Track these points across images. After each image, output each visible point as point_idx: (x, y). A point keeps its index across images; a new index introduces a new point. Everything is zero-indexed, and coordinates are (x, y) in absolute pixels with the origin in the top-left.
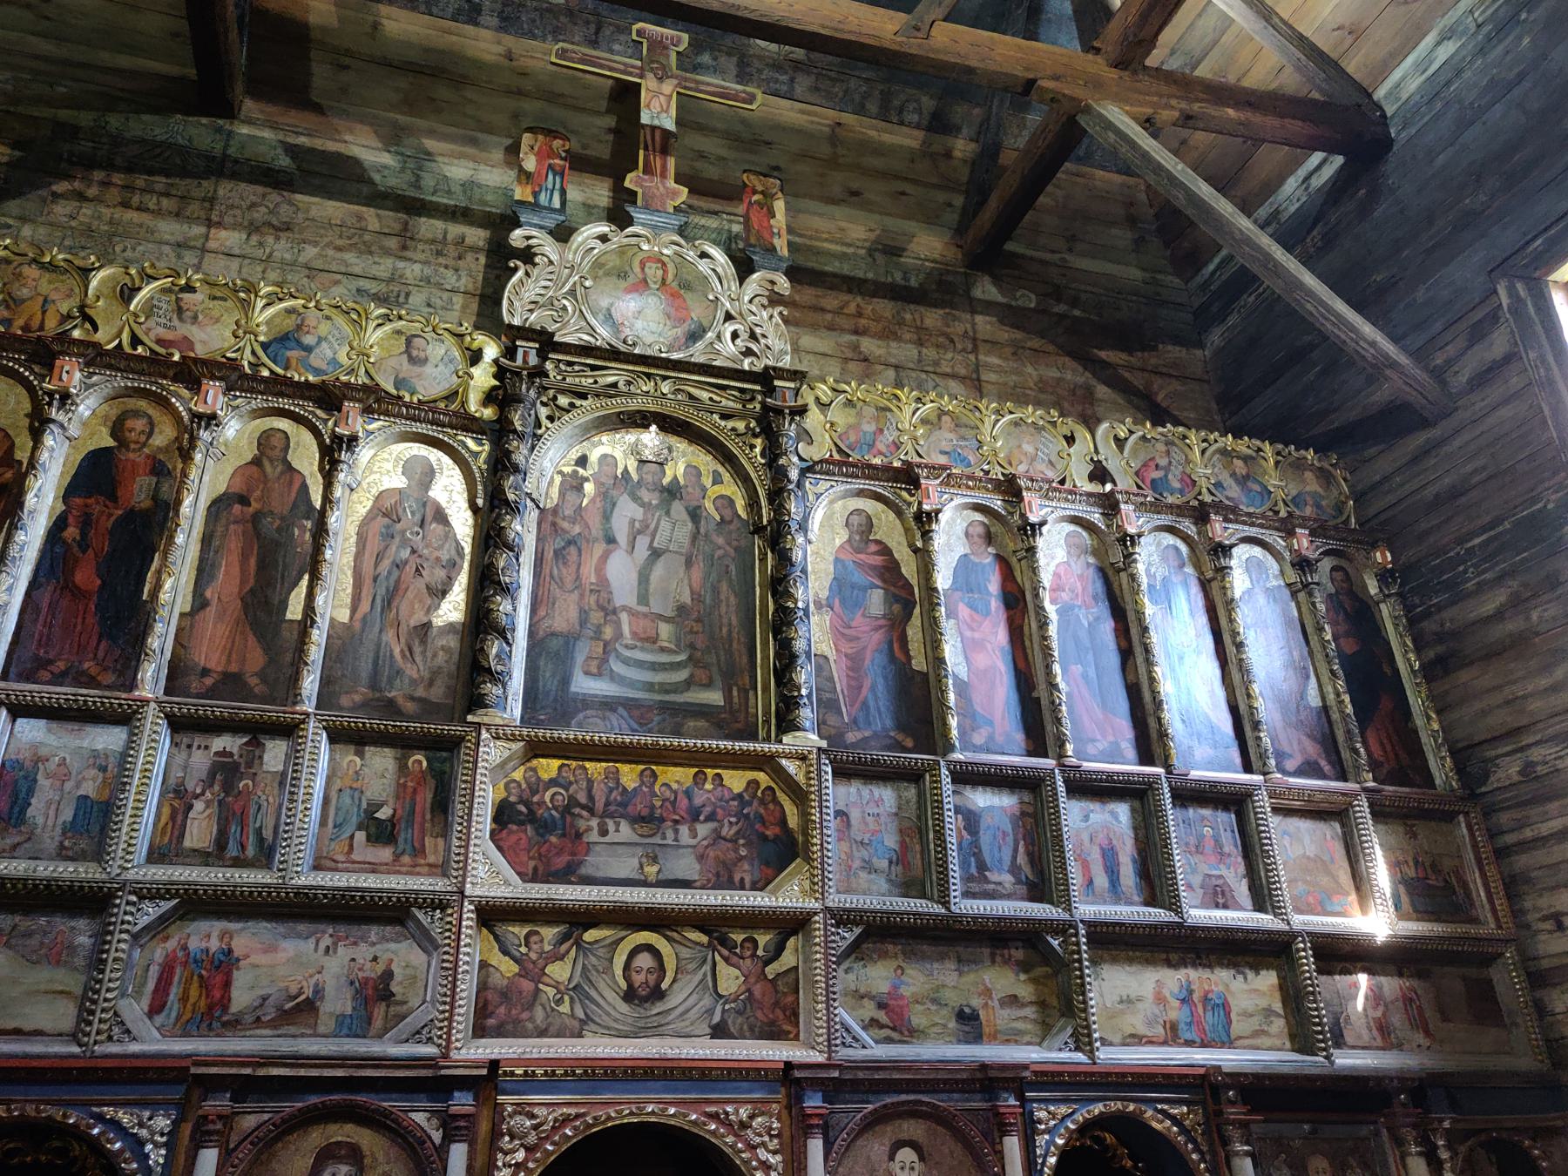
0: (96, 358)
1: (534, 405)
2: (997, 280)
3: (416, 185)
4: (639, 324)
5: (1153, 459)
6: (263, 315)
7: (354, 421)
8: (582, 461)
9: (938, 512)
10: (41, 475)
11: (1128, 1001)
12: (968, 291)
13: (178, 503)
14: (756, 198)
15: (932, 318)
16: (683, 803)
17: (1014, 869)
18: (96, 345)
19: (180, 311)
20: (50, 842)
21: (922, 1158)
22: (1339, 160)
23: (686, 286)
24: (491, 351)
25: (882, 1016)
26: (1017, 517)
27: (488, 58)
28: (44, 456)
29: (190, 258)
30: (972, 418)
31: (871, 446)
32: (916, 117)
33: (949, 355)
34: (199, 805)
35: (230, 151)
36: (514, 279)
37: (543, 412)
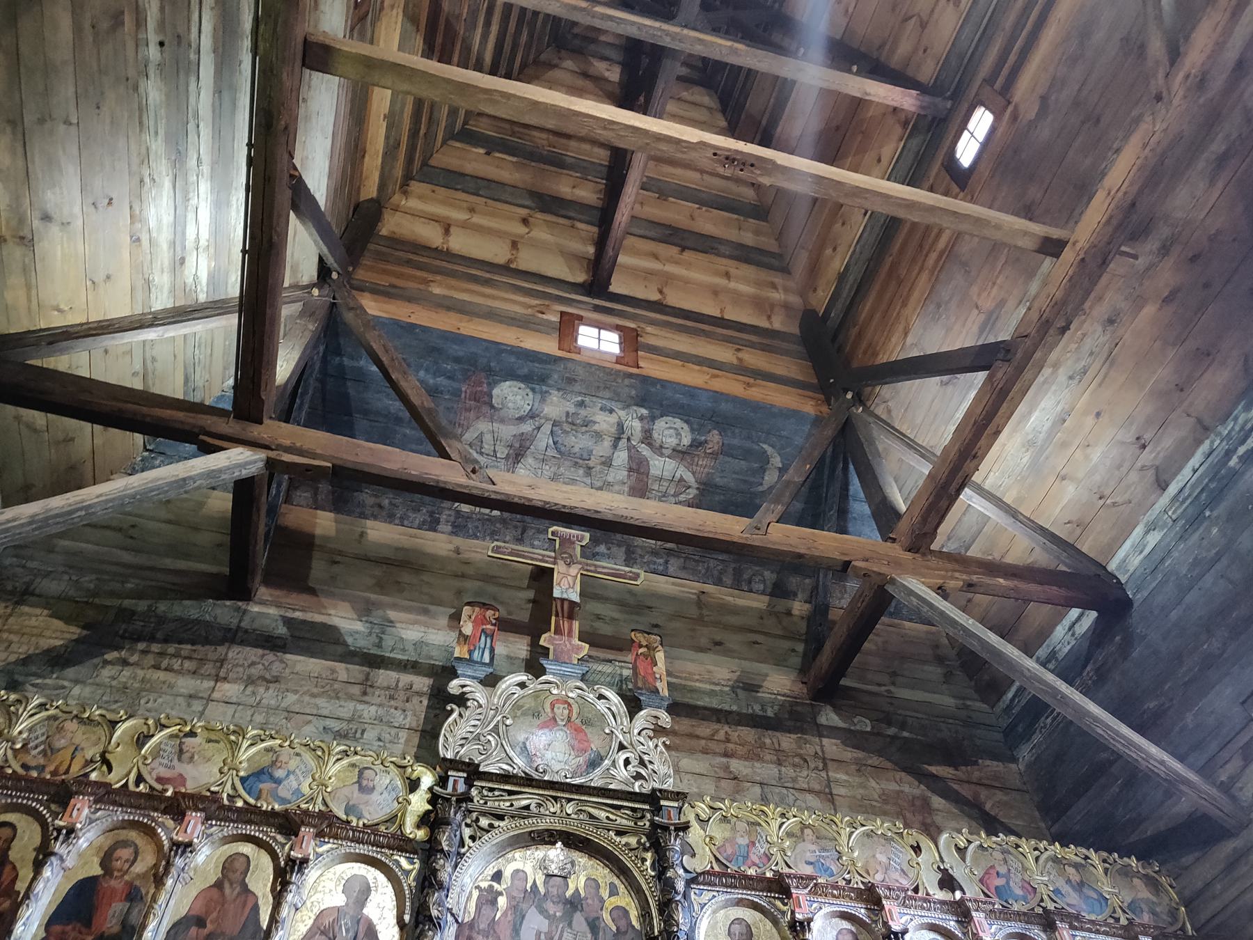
0: (105, 795)
1: (460, 826)
2: (837, 709)
3: (379, 646)
4: (549, 755)
5: (992, 867)
6: (247, 754)
7: (309, 845)
8: (497, 876)
9: (810, 920)
10: (33, 905)
12: (815, 718)
13: (143, 927)
14: (641, 650)
15: (787, 741)
18: (107, 785)
19: (181, 751)
22: (1093, 615)
23: (587, 722)
24: (428, 780)
26: (880, 925)
27: (444, 553)
28: (40, 886)
29: (197, 706)
30: (830, 831)
31: (746, 857)
32: (762, 587)
33: (805, 773)
35: (242, 624)
36: (451, 719)
37: (467, 832)
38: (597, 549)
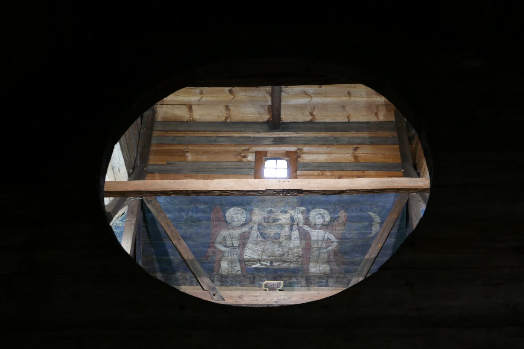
38: (292, 281)
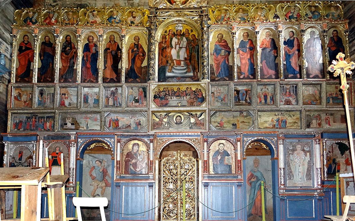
1: (155, 23)
5: (290, 11)
11: (266, 122)
16: (185, 93)
17: (246, 100)
19: (93, 15)
20: (92, 105)
21: (224, 146)
25: (219, 125)
28: (79, 47)
34: (110, 99)
